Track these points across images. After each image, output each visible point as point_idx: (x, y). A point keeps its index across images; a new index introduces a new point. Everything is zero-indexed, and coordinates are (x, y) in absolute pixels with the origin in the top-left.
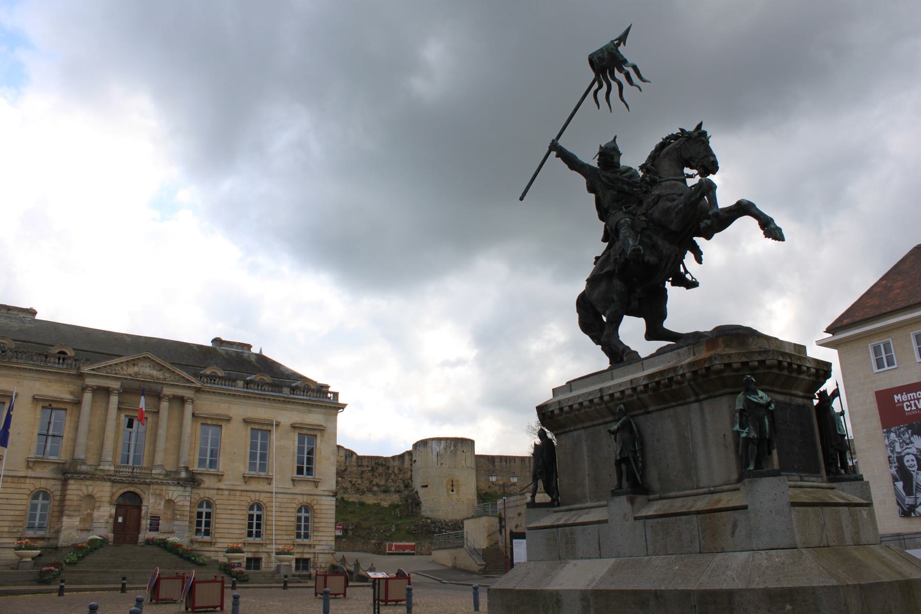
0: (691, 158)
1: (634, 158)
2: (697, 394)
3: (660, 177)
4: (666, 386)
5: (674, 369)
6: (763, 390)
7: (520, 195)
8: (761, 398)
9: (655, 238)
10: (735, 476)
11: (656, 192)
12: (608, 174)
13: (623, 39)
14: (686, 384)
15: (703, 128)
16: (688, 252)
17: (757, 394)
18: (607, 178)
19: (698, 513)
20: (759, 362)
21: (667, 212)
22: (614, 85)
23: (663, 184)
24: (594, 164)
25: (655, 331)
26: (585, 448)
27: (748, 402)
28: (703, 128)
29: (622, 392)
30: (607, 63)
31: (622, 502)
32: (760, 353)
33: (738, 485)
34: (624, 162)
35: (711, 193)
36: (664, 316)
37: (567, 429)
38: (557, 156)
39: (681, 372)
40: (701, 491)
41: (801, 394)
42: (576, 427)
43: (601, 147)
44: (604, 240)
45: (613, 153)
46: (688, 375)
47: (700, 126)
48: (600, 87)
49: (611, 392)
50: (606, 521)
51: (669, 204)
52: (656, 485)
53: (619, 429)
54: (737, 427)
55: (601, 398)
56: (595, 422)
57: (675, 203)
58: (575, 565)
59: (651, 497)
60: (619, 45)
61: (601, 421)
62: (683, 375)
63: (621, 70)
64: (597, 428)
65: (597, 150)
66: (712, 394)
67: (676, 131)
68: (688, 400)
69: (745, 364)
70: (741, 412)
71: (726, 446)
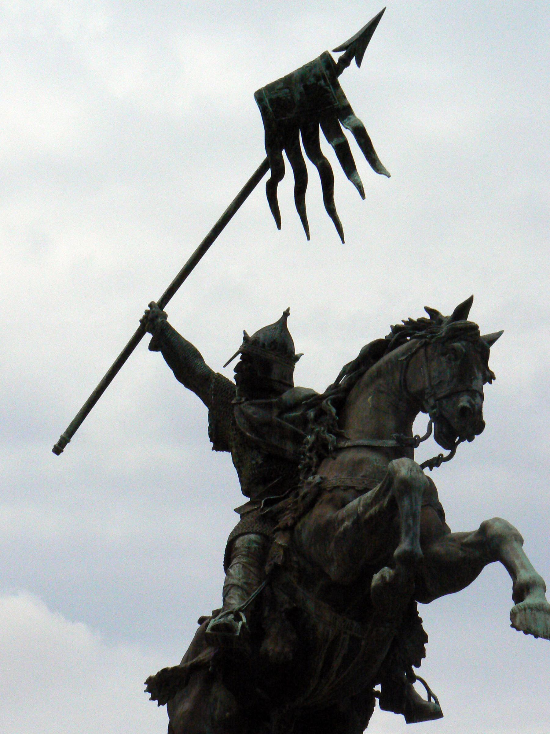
7: (56, 440)
9: (301, 592)
13: (356, 49)
15: (472, 317)
21: (325, 531)
28: (472, 317)
38: (153, 347)
43: (246, 338)
45: (270, 355)
47: (464, 309)
48: (278, 175)
60: (345, 62)
67: (419, 314)
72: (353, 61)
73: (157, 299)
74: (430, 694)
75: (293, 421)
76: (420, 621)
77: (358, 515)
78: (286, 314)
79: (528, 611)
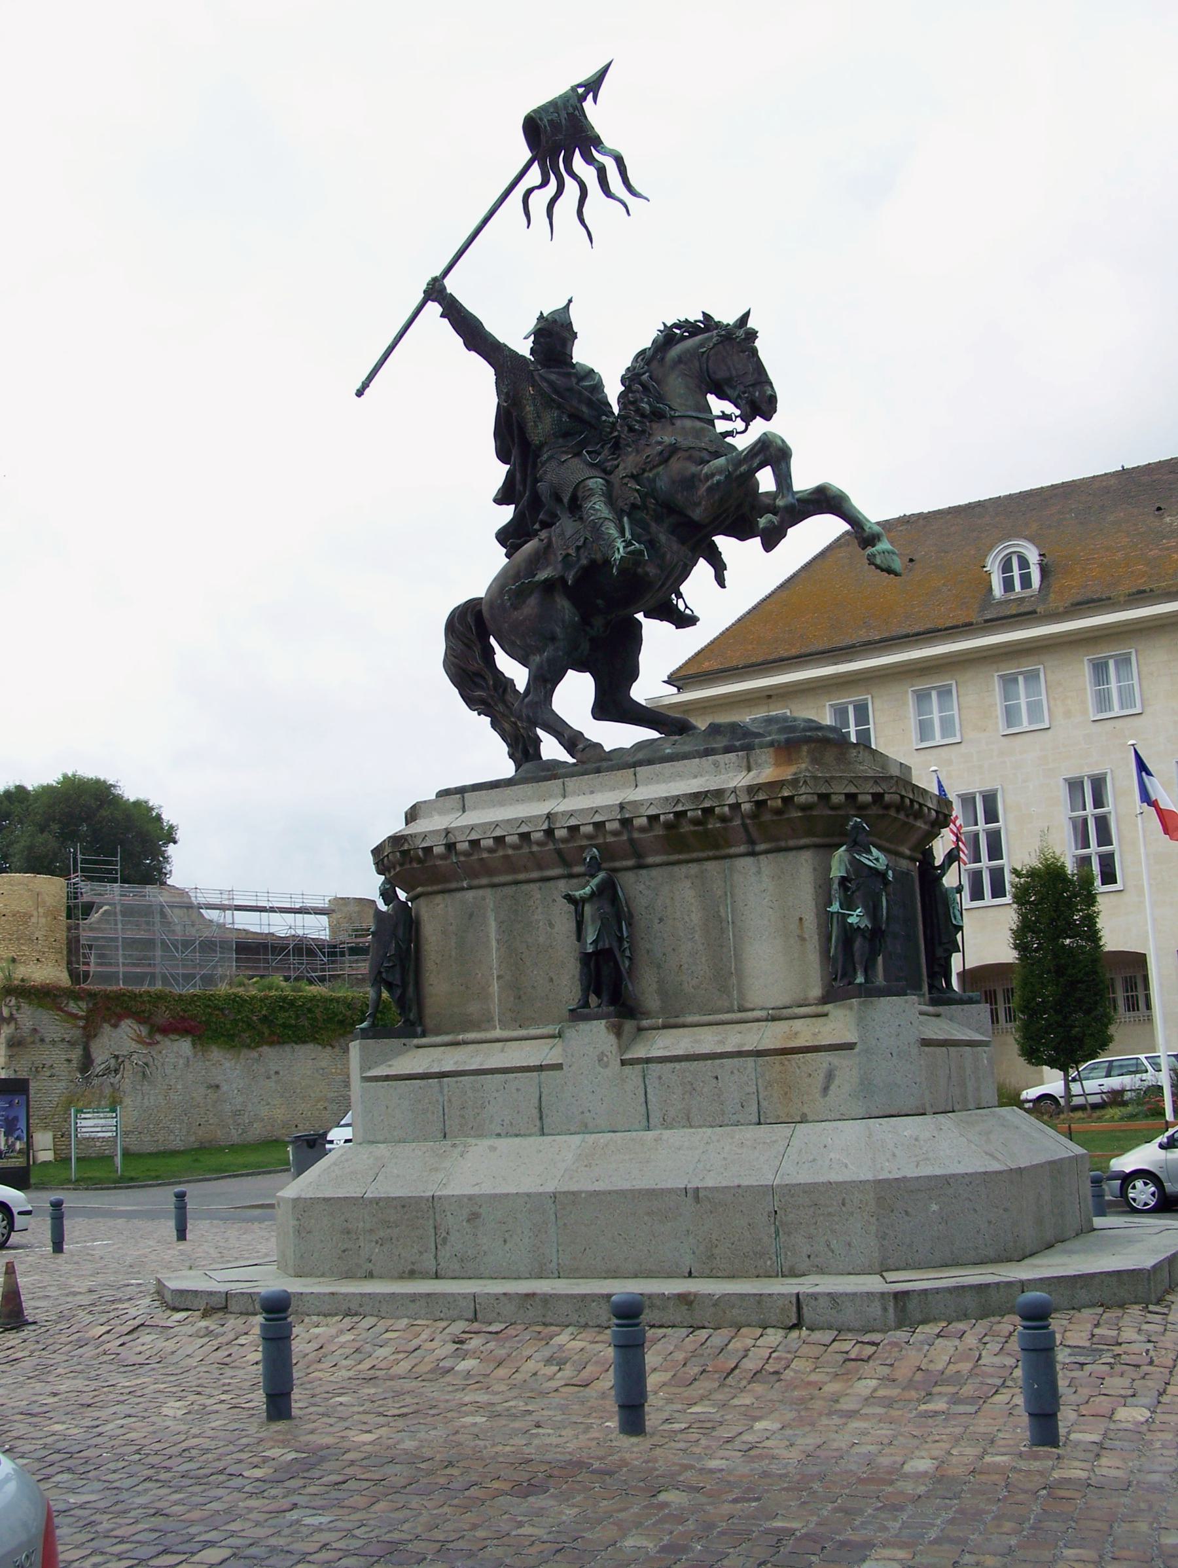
0: (729, 381)
1: (607, 354)
2: (752, 842)
4: (696, 822)
5: (719, 793)
6: (879, 848)
7: (358, 385)
8: (877, 860)
10: (816, 992)
11: (668, 439)
12: (553, 377)
14: (737, 822)
16: (701, 560)
17: (870, 852)
18: (551, 384)
19: (759, 1054)
21: (690, 483)
22: (571, 185)
23: (678, 423)
24: (524, 348)
25: (613, 703)
26: (493, 925)
27: (857, 865)
28: (751, 324)
29: (599, 826)
30: (559, 135)
31: (596, 1035)
32: (876, 780)
33: (828, 1008)
34: (582, 354)
36: (633, 674)
37: (454, 885)
39: (732, 800)
40: (750, 1015)
41: (907, 852)
42: (476, 882)
44: (503, 498)
46: (746, 807)
47: (746, 316)
48: (545, 183)
49: (573, 822)
50: (559, 1067)
51: (694, 469)
52: (652, 1002)
53: (593, 894)
54: (835, 907)
55: (549, 832)
56: (522, 876)
57: (706, 469)
58: (493, 1149)
59: (645, 1023)
61: (535, 875)
62: (736, 807)
63: (589, 159)
64: (525, 887)
65: (531, 324)
66: (783, 844)
67: (694, 316)
68: (733, 850)
69: (851, 797)
70: (843, 881)
71: (803, 939)
72: (591, 96)
73: (437, 273)
74: (687, 607)
75: (586, 388)
78: (570, 301)
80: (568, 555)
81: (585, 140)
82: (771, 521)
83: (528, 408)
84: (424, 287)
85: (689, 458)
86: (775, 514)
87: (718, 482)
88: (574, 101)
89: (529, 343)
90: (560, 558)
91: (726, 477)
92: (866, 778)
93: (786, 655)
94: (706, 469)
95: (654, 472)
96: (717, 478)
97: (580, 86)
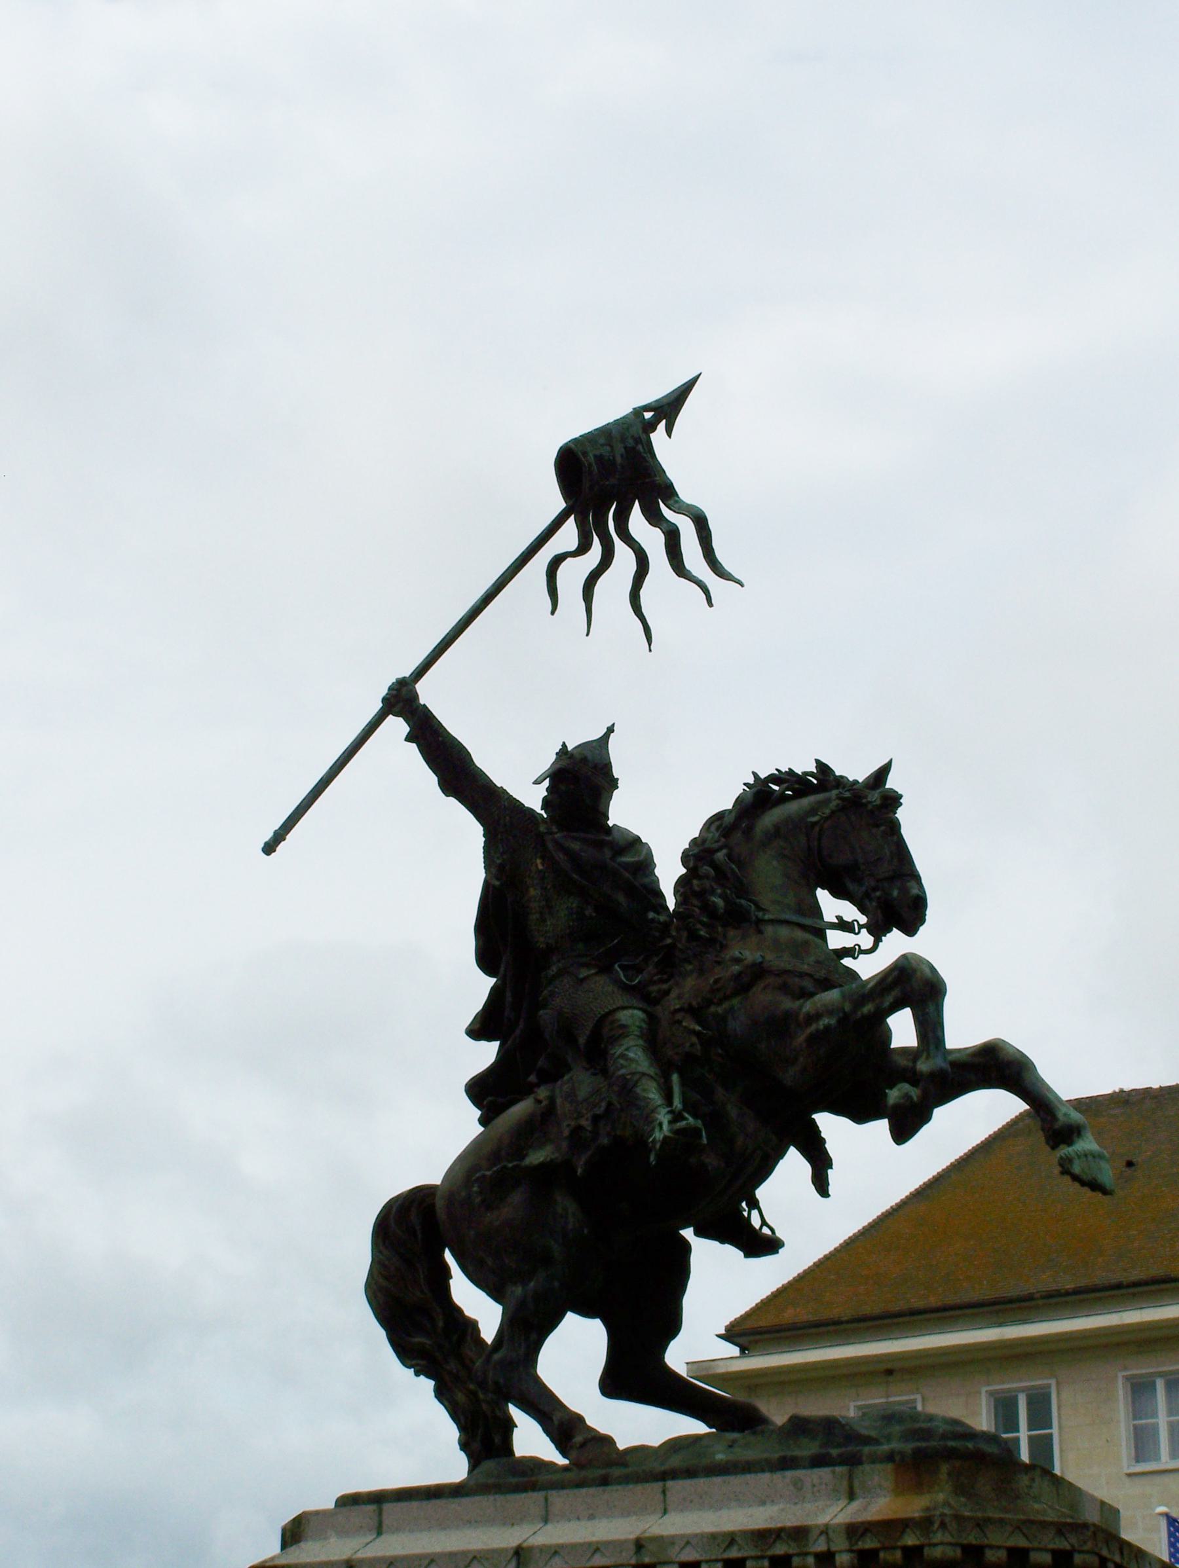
1: (663, 814)
3: (759, 908)
5: (799, 1533)
7: (268, 835)
9: (720, 1093)
12: (576, 846)
15: (892, 783)
18: (572, 856)
20: (1055, 1553)
21: (781, 1025)
22: (624, 556)
23: (769, 930)
24: (533, 797)
25: (634, 1371)
28: (892, 783)
30: (611, 477)
32: (1061, 1529)
34: (624, 812)
35: (931, 1008)
36: (671, 1325)
38: (409, 738)
39: (821, 1546)
44: (480, 1029)
47: (882, 773)
48: (583, 548)
51: (788, 1004)
57: (808, 1006)
60: (651, 426)
63: (654, 517)
65: (546, 760)
67: (804, 765)
72: (662, 426)
73: (406, 672)
74: (764, 1223)
75: (626, 866)
76: (823, 1141)
77: (845, 1013)
78: (611, 730)
79: (1090, 1158)
80: (579, 1128)
81: (649, 487)
82: (907, 1096)
83: (532, 892)
84: (384, 691)
85: (784, 988)
86: (914, 1083)
87: (827, 1028)
88: (637, 430)
89: (542, 790)
90: (566, 1133)
91: (839, 1022)
92: (1044, 1525)
93: (919, 1304)
94: (808, 1006)
95: (726, 1005)
96: (825, 1021)
97: (647, 408)
